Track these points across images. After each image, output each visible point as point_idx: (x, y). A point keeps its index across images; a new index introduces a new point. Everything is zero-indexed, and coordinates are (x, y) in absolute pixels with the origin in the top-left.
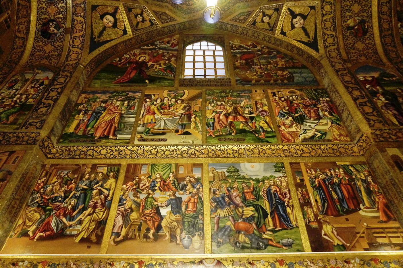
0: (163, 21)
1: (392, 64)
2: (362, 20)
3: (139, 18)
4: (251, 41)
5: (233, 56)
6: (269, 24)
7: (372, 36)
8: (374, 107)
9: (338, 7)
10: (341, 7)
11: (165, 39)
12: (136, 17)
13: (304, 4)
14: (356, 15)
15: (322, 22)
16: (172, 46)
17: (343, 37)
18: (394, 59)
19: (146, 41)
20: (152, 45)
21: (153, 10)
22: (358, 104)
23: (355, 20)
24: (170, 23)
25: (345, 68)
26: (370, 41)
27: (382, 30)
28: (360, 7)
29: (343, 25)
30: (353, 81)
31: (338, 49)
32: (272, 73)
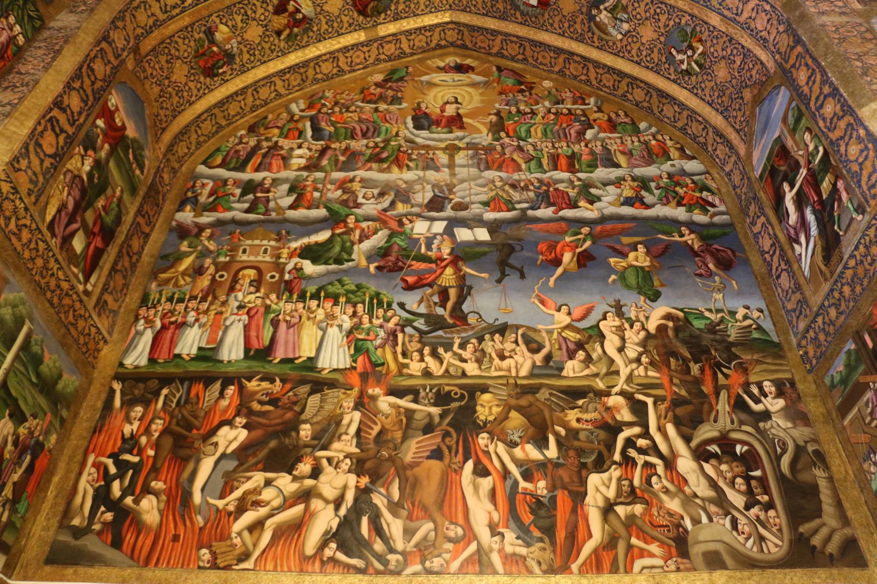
1: (165, 155)
2: (234, 55)
7: (206, 91)
8: (60, 157)
14: (239, 39)
17: (187, 28)
18: (174, 154)
22: (51, 114)
23: (229, 39)
25: (120, 55)
26: (195, 92)
27: (224, 104)
28: (257, 42)
29: (213, 17)
30: (99, 84)
31: (158, 24)
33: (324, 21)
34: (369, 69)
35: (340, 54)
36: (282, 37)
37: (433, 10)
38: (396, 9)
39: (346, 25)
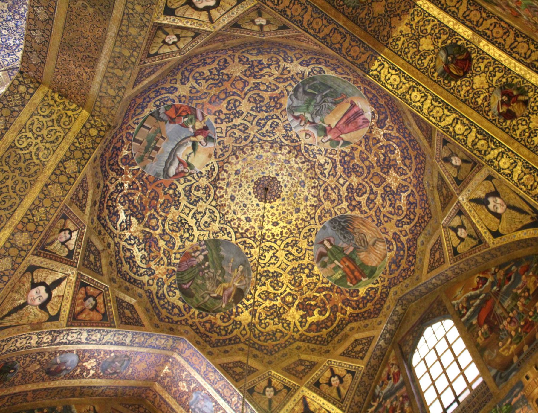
0: (361, 355)
3: (335, 381)
4: (475, 274)
5: (469, 329)
6: (470, 236)
9: (514, 147)
10: (519, 142)
11: (383, 375)
12: (330, 384)
13: (477, 182)
15: (517, 186)
16: (395, 380)
19: (364, 400)
20: (374, 401)
21: (340, 355)
24: (371, 349)
32: (530, 317)
33: (495, 79)
34: (499, 15)
35: (506, 47)
36: (526, 98)
37: (427, 14)
38: (448, 39)
39: (486, 61)
